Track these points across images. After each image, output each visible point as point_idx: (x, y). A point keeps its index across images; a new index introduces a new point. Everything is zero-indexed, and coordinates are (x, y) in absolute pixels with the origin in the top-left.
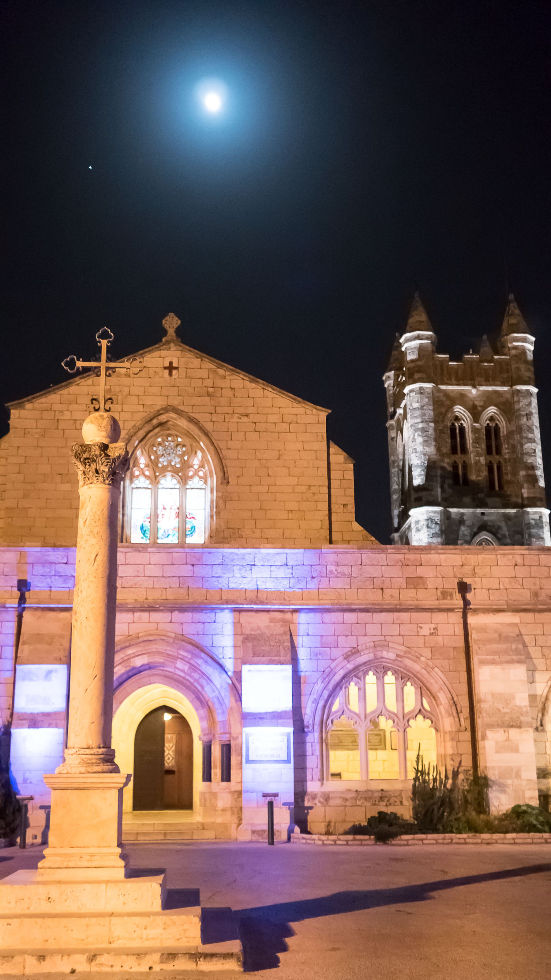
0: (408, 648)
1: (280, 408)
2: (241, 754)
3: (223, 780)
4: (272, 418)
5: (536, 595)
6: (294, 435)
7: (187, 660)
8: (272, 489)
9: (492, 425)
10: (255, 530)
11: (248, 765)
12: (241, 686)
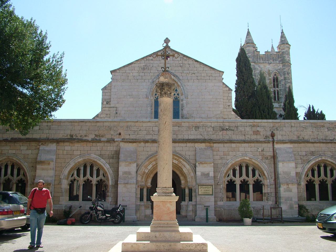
2: (195, 192)
3: (189, 201)
4: (203, 75)
5: (298, 137)
7: (177, 160)
9: (275, 77)
10: (198, 115)
11: (198, 196)
12: (196, 169)
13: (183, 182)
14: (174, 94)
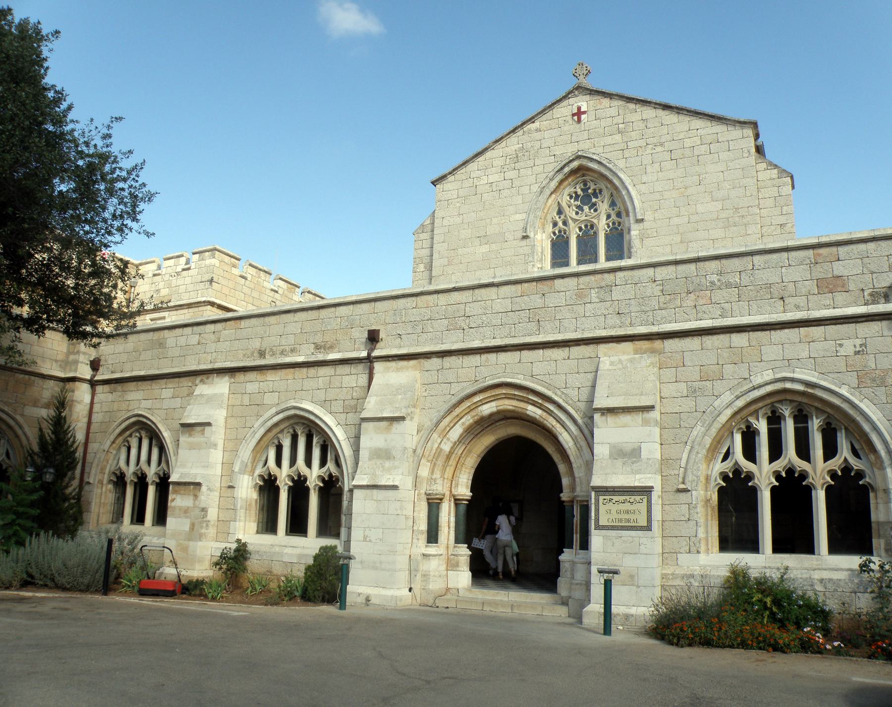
0: (823, 374)
1: (697, 129)
4: (688, 143)
6: (716, 155)
8: (694, 218)
13: (565, 481)
14: (609, 217)
